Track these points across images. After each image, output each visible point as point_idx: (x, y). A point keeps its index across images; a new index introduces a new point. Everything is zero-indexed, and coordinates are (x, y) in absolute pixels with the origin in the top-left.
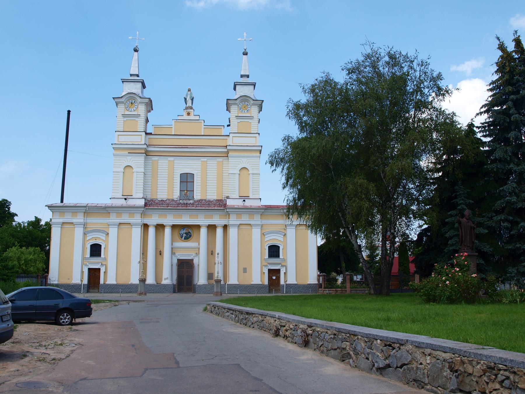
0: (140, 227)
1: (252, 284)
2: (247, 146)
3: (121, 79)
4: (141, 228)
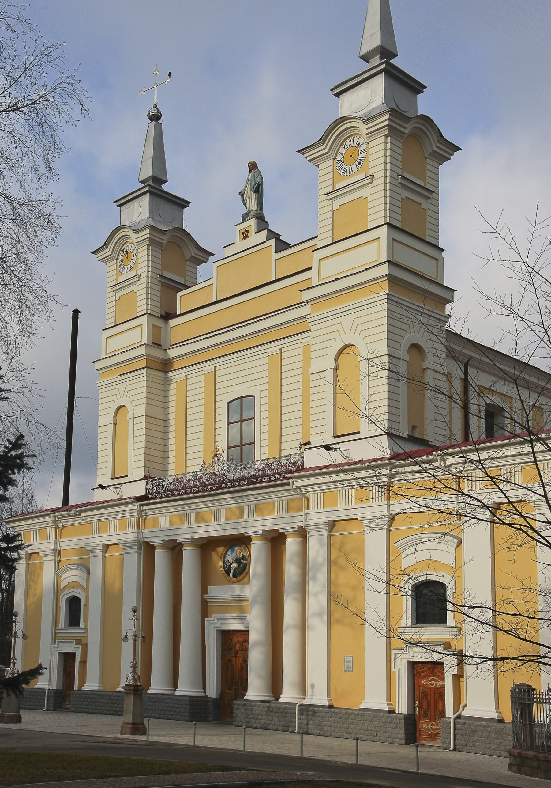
0: (136, 550)
1: (361, 709)
2: (351, 275)
3: (115, 202)
4: (139, 553)
